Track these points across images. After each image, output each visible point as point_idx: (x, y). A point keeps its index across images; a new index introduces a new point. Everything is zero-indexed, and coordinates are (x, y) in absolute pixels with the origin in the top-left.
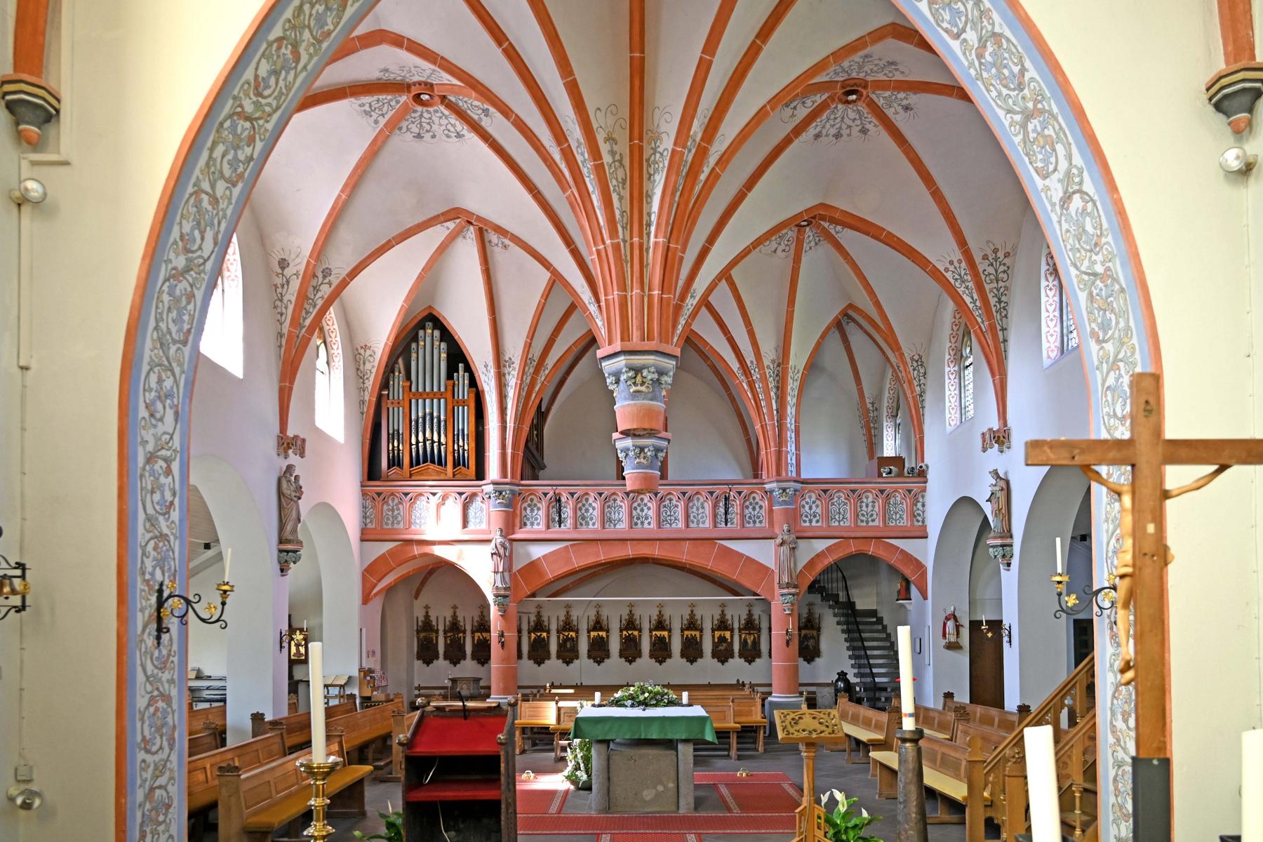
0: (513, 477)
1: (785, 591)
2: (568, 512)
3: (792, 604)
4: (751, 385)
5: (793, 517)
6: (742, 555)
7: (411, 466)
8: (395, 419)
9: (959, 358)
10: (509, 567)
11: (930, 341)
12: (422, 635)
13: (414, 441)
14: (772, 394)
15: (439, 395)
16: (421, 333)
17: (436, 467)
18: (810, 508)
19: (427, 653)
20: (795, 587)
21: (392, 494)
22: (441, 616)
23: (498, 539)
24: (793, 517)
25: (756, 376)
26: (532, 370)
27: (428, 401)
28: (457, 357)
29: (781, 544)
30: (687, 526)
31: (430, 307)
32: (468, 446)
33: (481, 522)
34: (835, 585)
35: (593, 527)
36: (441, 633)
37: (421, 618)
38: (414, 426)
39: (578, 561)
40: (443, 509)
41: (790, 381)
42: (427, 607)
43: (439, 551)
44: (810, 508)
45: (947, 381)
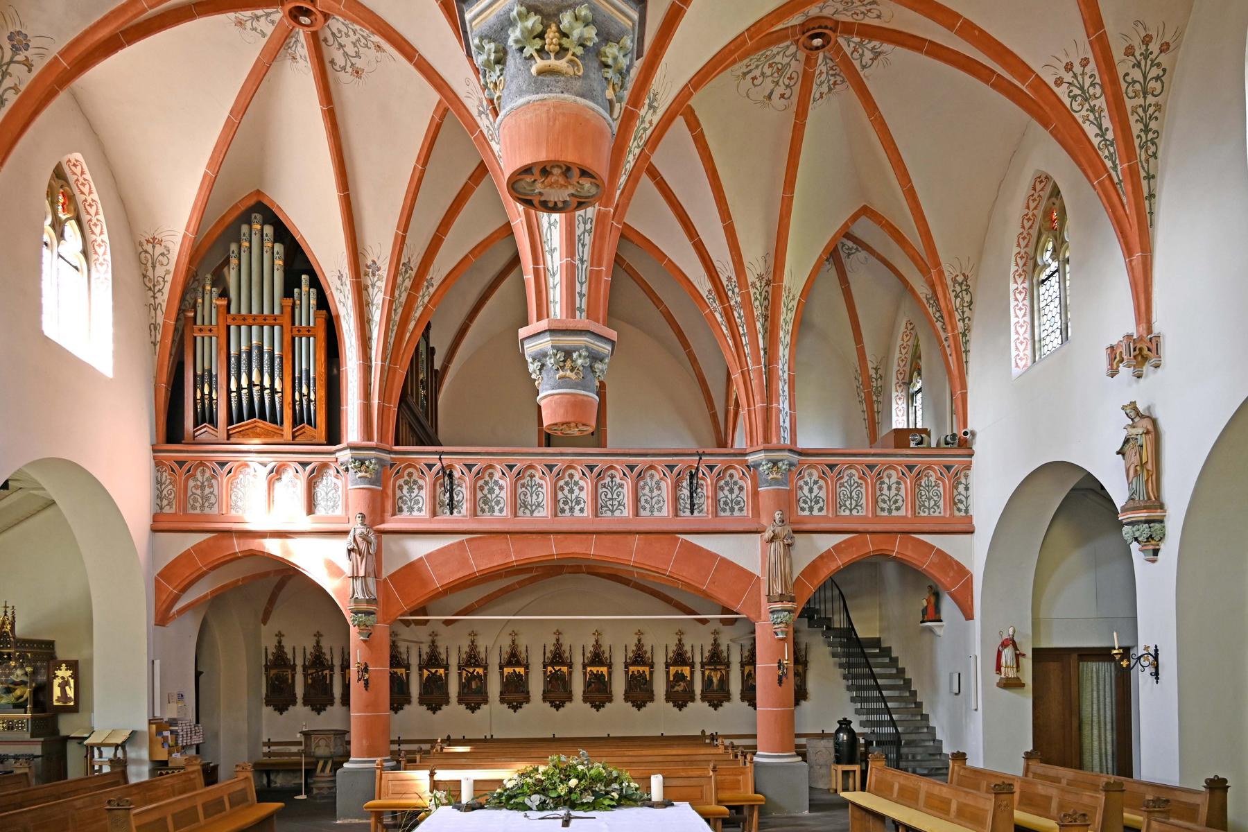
0: (381, 439)
1: (778, 606)
2: (463, 493)
3: (787, 625)
4: (728, 313)
5: (787, 501)
6: (714, 556)
7: (230, 422)
8: (208, 354)
9: (1031, 267)
10: (375, 571)
11: (981, 253)
12: (273, 672)
13: (233, 387)
14: (759, 325)
15: (273, 321)
17: (268, 425)
18: (811, 491)
19: (280, 697)
20: (792, 600)
21: (201, 464)
22: (299, 646)
23: (356, 527)
24: (787, 501)
25: (735, 299)
26: (408, 283)
27: (254, 328)
28: (298, 265)
29: (772, 540)
30: (637, 514)
31: (258, 192)
32: (316, 395)
33: (335, 506)
34: (829, 606)
35: (500, 515)
36: (299, 670)
37: (272, 649)
38: (233, 365)
39: (478, 563)
40: (278, 485)
41: (784, 309)
42: (280, 635)
43: (273, 547)
44: (811, 491)
45: (1013, 303)
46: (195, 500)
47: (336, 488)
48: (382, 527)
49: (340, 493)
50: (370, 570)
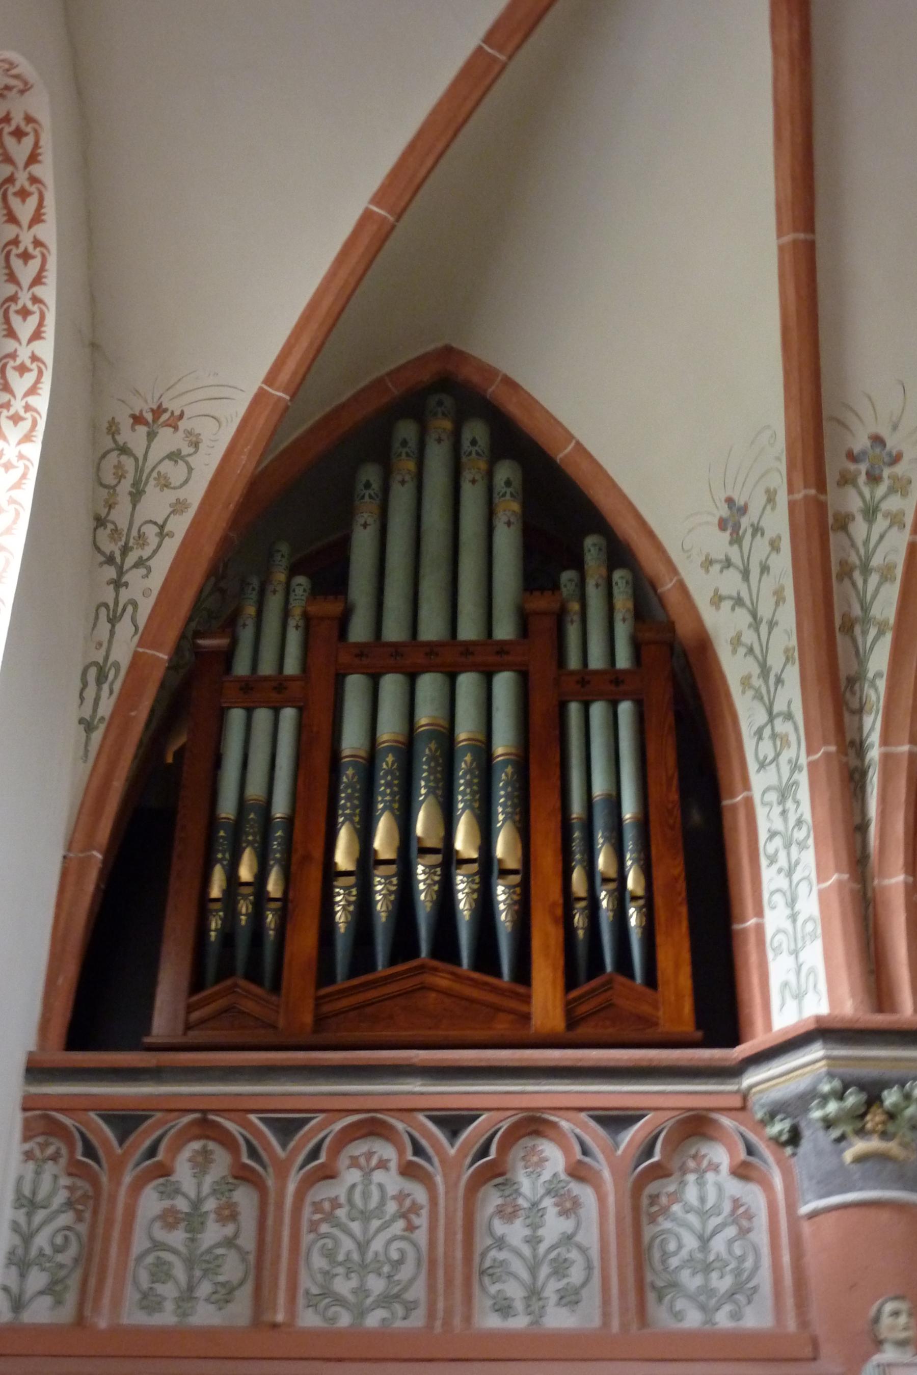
15: (485, 659)
16: (406, 430)
46: (161, 1272)
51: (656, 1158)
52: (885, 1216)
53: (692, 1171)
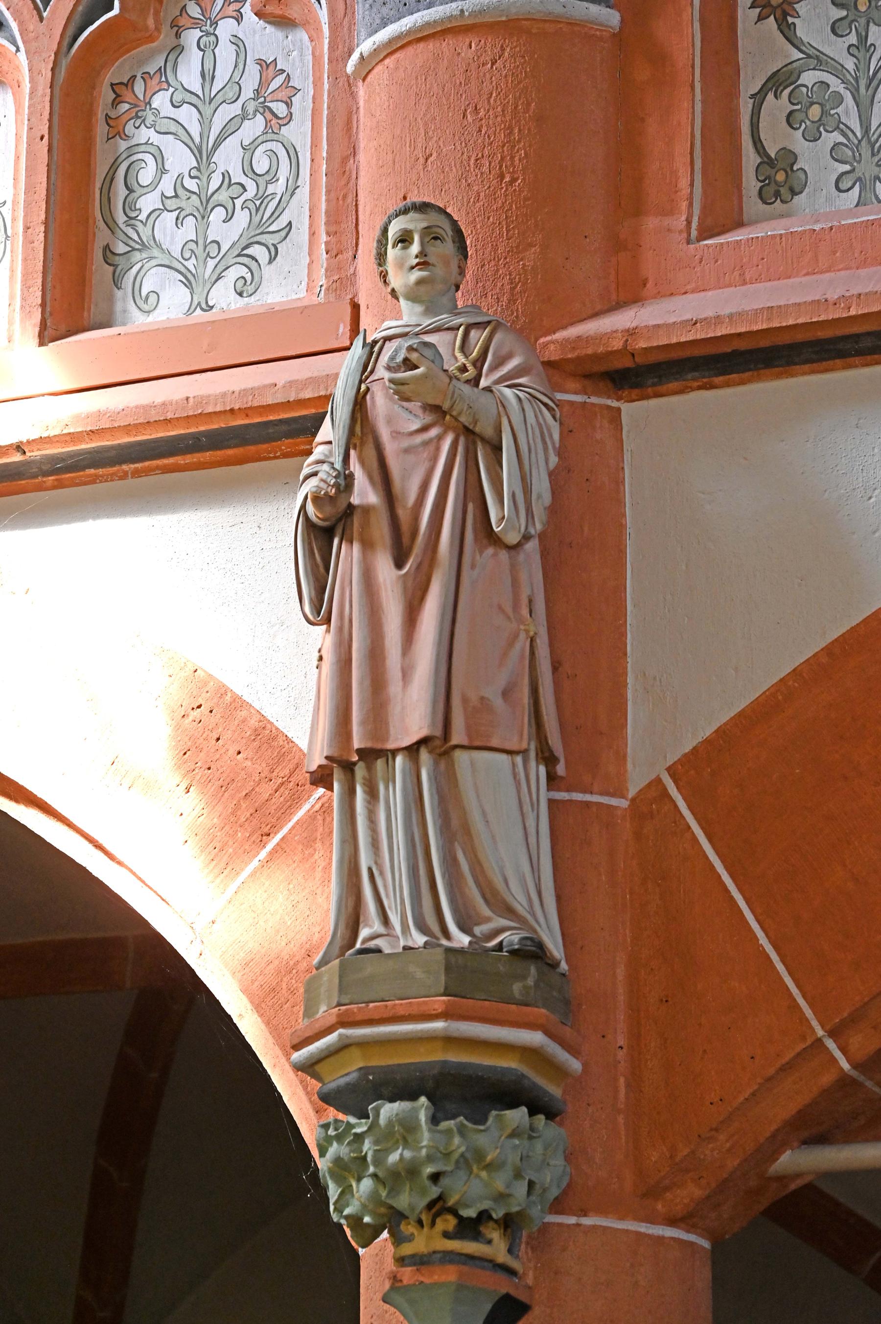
10: (571, 724)
33: (264, 237)
47: (270, 98)
48: (611, 327)
49: (298, 133)
50: (489, 679)
51: (116, 11)
52: (468, 49)
53: (196, 24)
